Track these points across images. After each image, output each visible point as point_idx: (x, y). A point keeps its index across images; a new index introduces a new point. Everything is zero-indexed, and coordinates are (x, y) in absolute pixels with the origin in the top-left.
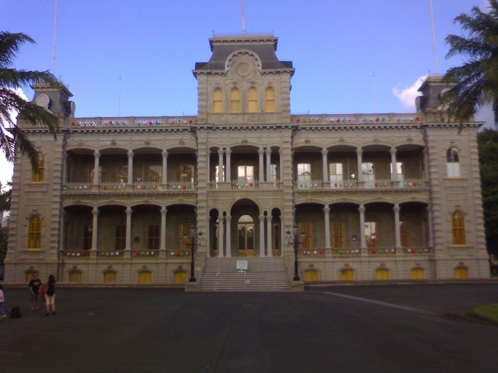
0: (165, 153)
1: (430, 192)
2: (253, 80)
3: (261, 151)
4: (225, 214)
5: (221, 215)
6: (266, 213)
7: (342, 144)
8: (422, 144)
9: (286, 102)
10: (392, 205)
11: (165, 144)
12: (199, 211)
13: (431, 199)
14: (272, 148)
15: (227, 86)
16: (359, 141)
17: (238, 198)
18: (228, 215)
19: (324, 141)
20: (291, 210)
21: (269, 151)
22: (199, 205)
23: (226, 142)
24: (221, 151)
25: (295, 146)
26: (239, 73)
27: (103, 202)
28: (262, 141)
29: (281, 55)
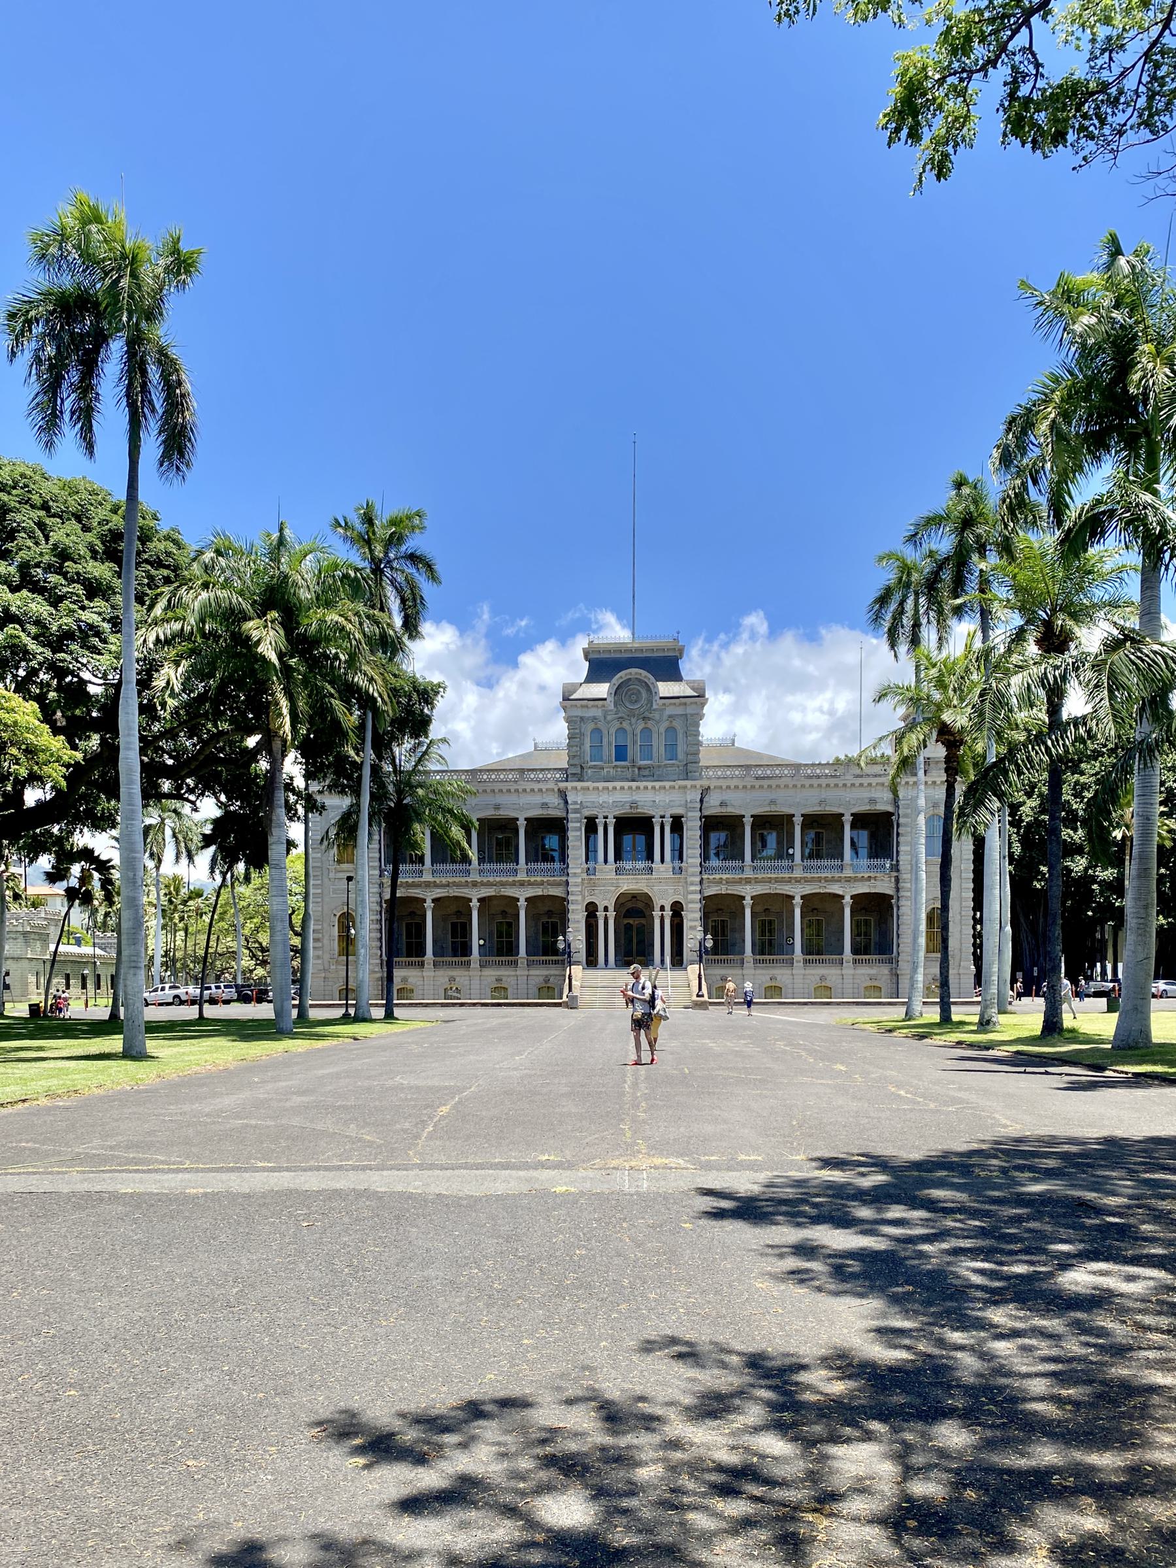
1: (897, 880)
3: (656, 821)
6: (662, 908)
7: (773, 808)
8: (890, 809)
9: (692, 749)
10: (842, 897)
12: (571, 907)
13: (898, 890)
15: (608, 723)
20: (698, 906)
21: (668, 821)
22: (570, 898)
24: (600, 821)
25: (706, 813)
26: (628, 705)
27: (439, 893)
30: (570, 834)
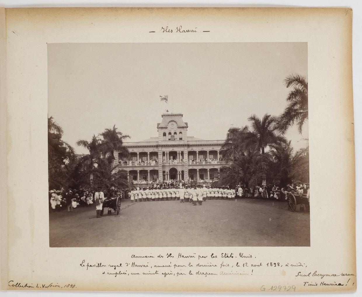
0: (148, 153)
2: (175, 130)
3: (178, 152)
4: (167, 172)
5: (166, 173)
6: (179, 172)
7: (203, 150)
11: (149, 150)
14: (181, 152)
16: (208, 149)
17: (171, 168)
18: (168, 173)
19: (197, 149)
21: (180, 152)
23: (168, 150)
24: (166, 152)
28: (178, 150)
29: (184, 119)
30: (159, 156)
